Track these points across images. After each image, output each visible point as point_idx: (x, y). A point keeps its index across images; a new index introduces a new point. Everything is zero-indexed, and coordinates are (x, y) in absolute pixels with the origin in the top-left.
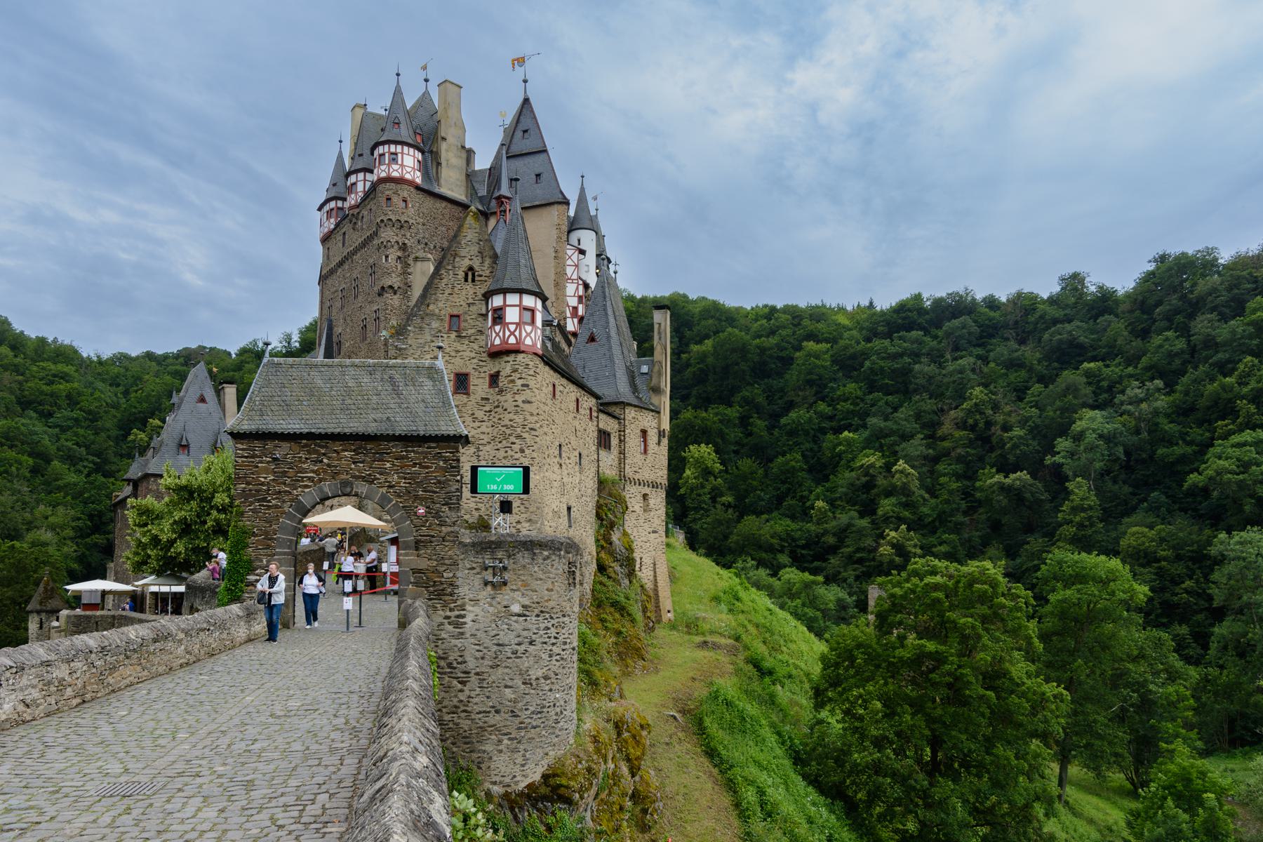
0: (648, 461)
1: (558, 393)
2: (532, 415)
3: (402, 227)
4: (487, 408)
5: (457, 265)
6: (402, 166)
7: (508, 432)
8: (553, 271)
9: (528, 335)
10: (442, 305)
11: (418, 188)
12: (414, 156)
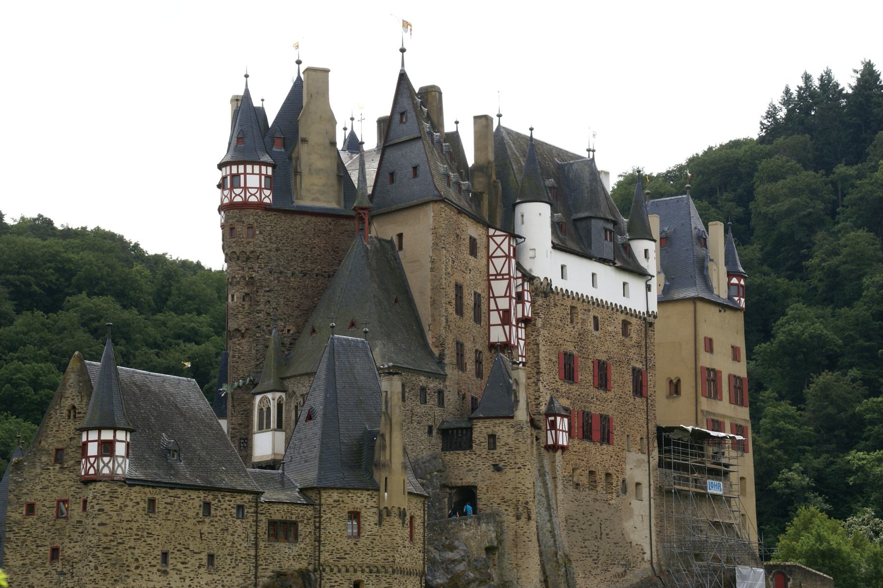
0: (360, 545)
1: (160, 506)
2: (106, 535)
3: (248, 258)
4: (80, 530)
5: (62, 405)
6: (246, 188)
8: (429, 287)
9: (106, 465)
12: (260, 174)
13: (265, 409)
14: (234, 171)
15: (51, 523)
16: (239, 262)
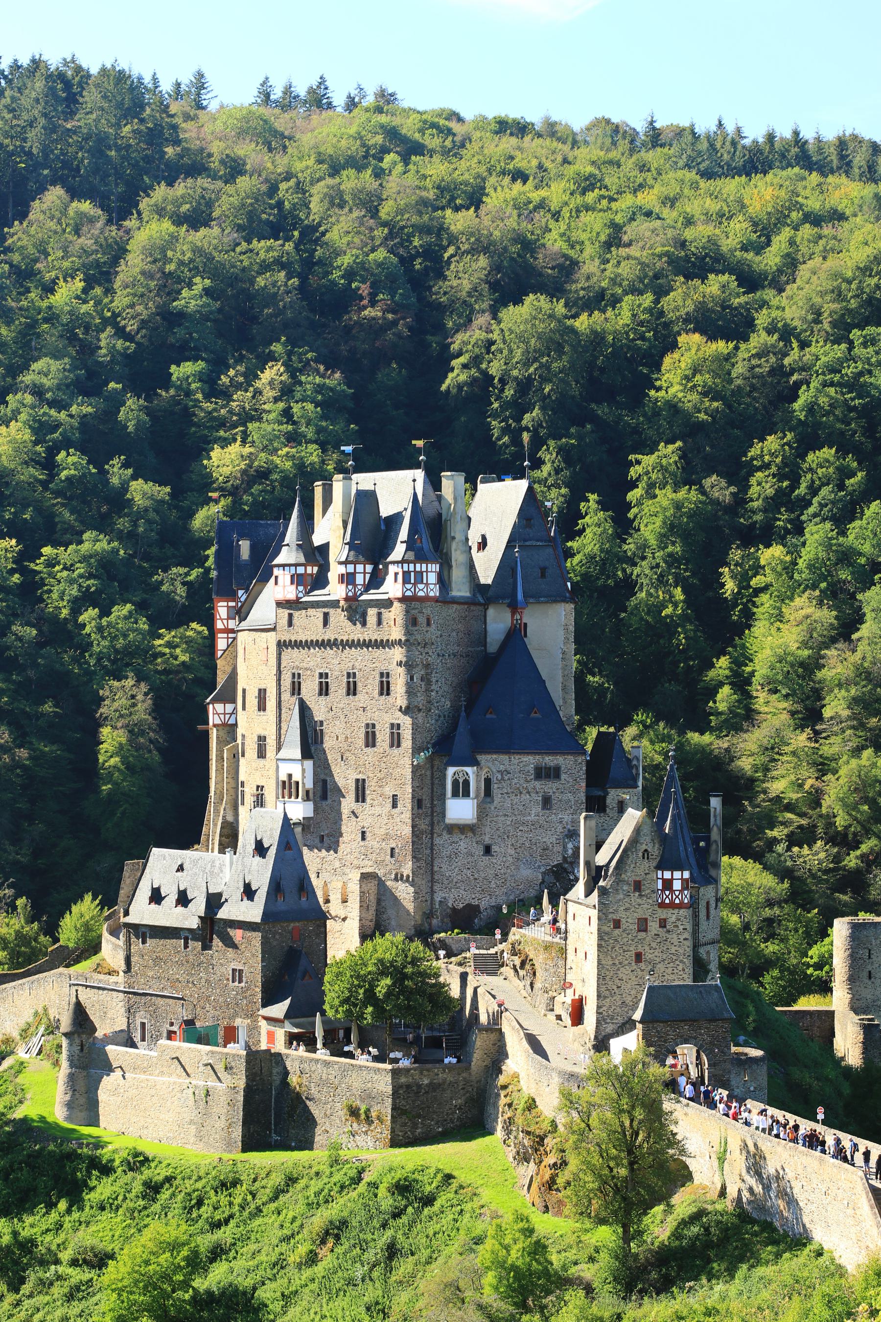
3: (426, 644)
6: (427, 584)
10: (629, 876)
11: (436, 600)
13: (461, 781)
14: (418, 569)
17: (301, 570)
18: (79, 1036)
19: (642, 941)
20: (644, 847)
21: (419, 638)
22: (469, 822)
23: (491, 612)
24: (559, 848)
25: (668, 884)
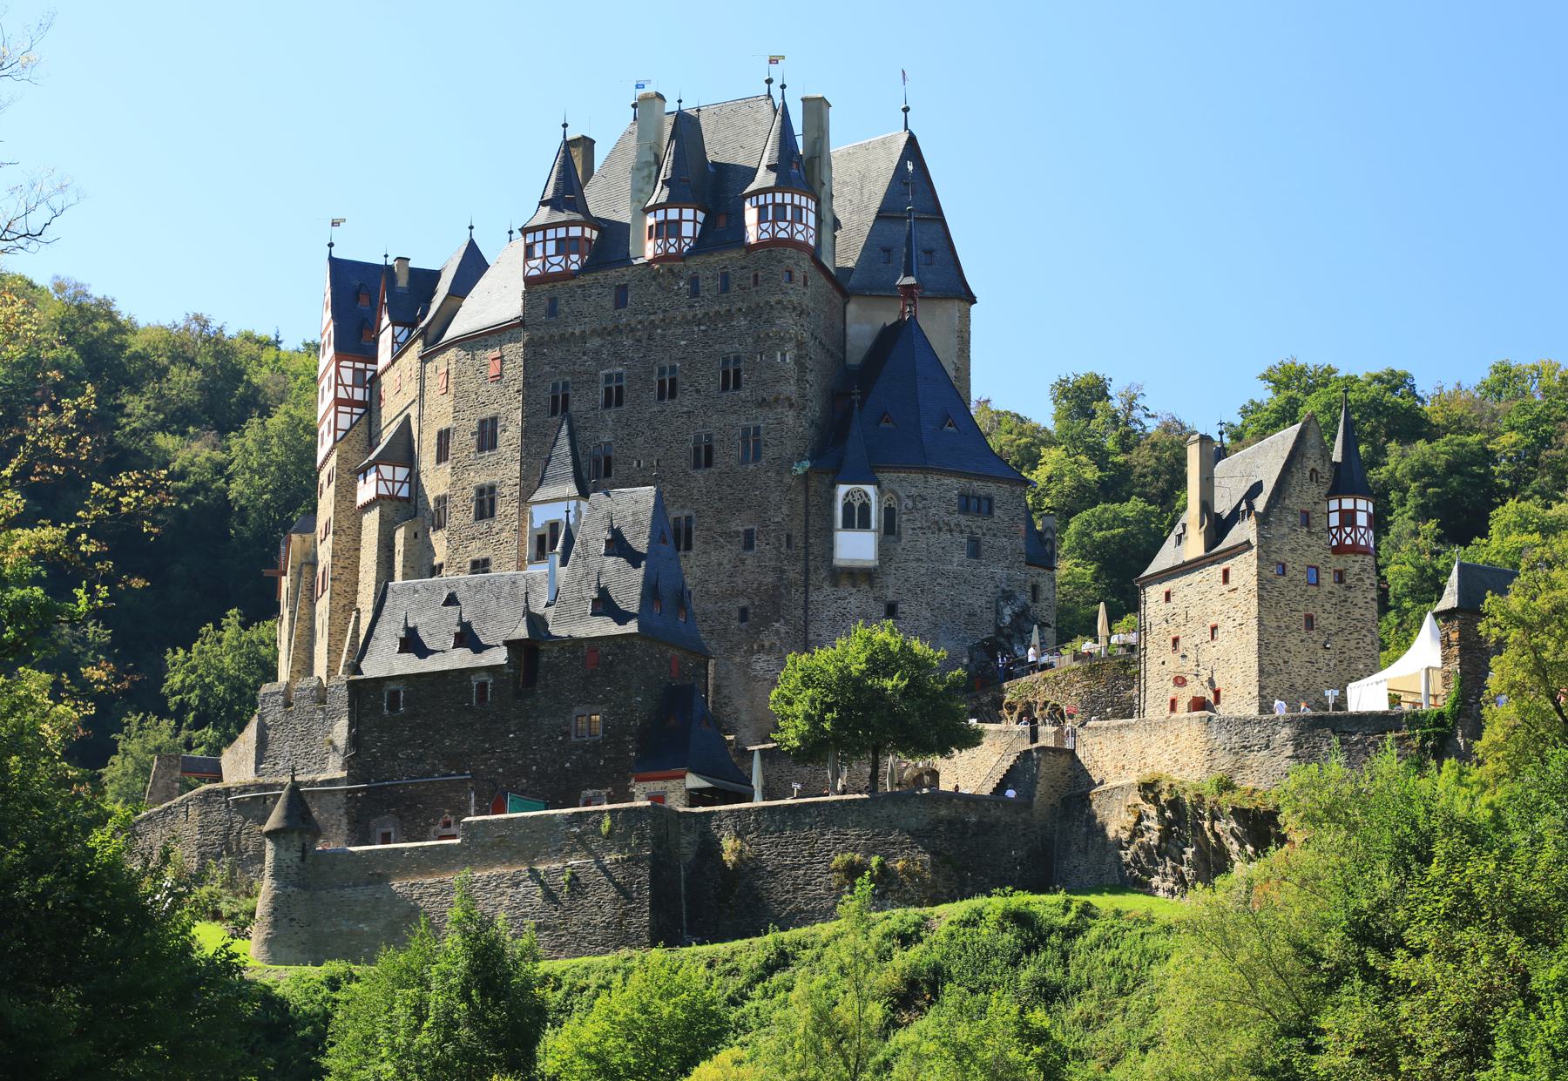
4: (1334, 601)
6: (806, 225)
7: (1360, 625)
13: (857, 505)
14: (796, 202)
15: (1304, 588)
16: (794, 314)
17: (575, 232)
18: (300, 835)
19: (1313, 598)
20: (1311, 464)
21: (794, 298)
22: (871, 564)
23: (852, 308)
24: (991, 616)
25: (1348, 518)
